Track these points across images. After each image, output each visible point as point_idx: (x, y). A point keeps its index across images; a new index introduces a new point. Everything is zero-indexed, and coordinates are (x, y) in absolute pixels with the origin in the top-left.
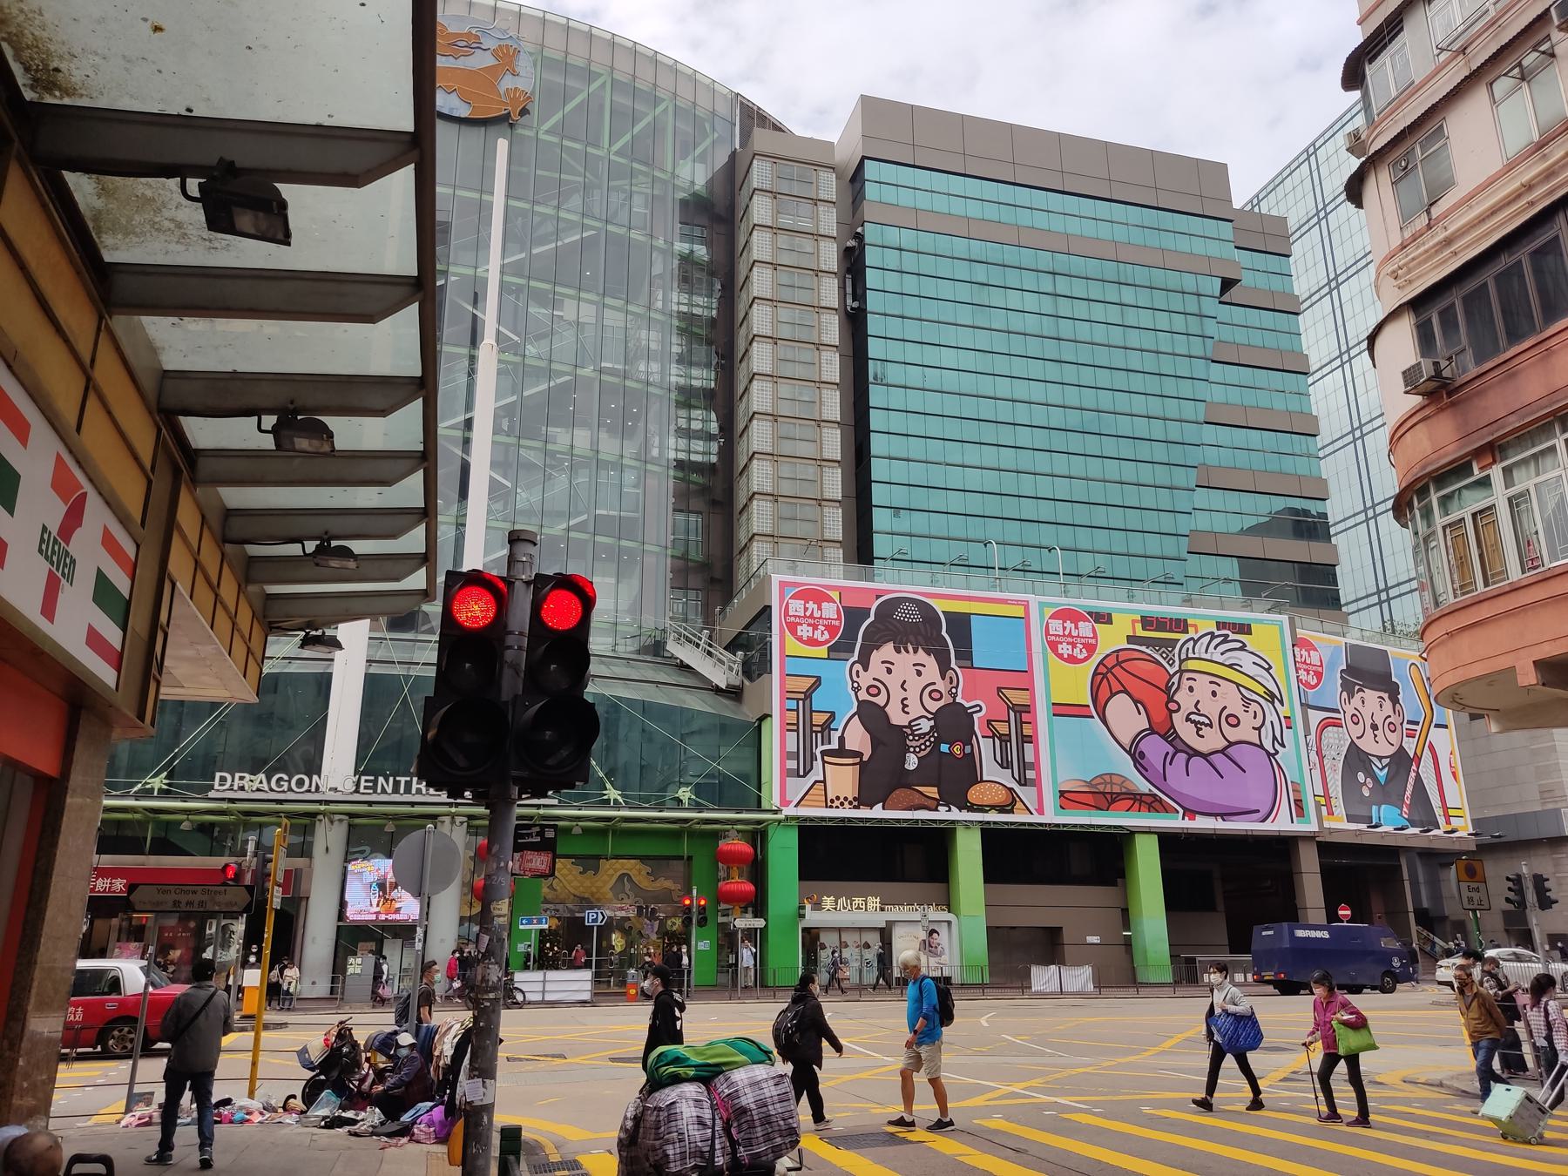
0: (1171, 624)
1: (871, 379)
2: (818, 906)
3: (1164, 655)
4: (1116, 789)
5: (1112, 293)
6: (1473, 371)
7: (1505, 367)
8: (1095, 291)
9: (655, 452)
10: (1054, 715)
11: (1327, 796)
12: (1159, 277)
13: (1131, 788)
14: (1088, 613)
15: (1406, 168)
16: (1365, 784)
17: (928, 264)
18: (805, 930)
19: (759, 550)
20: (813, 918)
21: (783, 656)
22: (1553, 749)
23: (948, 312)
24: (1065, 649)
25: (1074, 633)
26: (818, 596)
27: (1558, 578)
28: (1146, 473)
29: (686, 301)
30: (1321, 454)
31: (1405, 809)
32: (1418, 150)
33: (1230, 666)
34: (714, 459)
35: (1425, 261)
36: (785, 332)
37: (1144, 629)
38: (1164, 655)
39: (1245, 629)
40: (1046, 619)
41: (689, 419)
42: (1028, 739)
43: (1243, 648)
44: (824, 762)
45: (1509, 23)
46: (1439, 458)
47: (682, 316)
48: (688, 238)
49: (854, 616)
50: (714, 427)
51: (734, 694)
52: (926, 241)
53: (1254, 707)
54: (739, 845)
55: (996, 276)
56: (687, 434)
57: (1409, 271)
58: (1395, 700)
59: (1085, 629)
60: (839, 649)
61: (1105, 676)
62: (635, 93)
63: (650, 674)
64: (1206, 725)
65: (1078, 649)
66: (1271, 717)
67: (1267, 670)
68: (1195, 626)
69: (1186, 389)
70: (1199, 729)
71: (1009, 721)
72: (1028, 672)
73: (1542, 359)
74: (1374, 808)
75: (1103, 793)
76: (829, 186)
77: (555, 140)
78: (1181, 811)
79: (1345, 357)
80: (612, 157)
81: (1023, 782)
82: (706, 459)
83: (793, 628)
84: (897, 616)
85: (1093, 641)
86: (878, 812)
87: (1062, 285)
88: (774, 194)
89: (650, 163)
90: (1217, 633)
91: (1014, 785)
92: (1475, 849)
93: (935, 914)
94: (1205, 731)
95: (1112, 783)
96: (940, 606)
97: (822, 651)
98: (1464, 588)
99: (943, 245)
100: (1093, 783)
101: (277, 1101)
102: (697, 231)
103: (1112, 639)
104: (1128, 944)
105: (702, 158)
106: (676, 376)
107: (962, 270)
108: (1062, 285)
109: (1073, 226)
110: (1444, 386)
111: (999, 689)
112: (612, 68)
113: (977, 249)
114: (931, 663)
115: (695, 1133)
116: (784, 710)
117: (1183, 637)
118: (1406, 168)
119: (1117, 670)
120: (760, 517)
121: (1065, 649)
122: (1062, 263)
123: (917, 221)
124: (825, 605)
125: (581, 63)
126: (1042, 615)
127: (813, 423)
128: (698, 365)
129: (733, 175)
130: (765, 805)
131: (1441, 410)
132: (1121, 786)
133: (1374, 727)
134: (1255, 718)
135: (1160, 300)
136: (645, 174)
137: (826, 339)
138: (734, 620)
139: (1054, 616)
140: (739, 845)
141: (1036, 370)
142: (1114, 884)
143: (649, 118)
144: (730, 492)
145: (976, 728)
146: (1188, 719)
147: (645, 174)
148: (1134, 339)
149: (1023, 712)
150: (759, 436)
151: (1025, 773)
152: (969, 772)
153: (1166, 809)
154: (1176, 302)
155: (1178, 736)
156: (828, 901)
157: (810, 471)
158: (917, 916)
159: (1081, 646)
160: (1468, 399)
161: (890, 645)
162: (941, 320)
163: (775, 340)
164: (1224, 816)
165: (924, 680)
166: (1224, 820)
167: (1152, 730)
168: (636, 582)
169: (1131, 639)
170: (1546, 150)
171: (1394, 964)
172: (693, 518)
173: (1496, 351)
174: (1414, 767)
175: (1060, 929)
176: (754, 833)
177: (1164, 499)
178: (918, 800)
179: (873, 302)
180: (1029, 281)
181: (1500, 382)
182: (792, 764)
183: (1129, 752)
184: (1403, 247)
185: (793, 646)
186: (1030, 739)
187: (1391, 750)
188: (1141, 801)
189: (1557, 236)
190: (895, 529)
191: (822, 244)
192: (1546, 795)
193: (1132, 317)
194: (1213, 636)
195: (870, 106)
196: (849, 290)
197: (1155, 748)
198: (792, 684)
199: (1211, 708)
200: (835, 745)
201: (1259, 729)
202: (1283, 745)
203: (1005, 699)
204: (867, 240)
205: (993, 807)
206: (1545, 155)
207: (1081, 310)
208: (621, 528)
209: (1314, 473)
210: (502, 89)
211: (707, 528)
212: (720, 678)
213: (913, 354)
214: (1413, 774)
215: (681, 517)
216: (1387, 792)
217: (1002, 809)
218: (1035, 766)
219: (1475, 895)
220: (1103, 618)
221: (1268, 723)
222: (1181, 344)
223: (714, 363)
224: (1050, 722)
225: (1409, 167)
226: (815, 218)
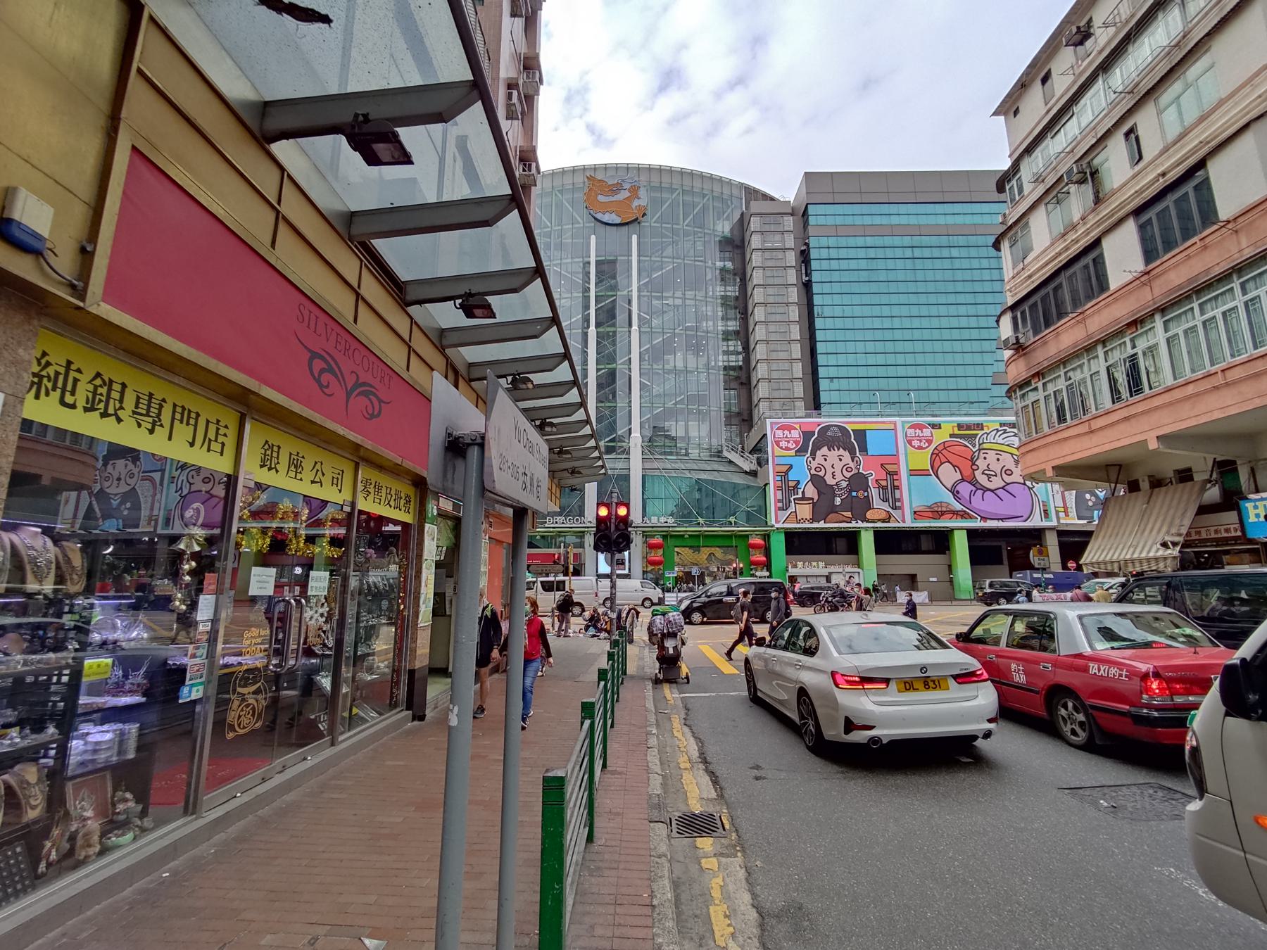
1: (816, 316)
2: (795, 566)
4: (944, 509)
5: (945, 253)
6: (1033, 340)
8: (936, 253)
9: (713, 363)
11: (1065, 507)
13: (953, 508)
14: (929, 425)
18: (789, 577)
19: (763, 406)
20: (792, 571)
24: (916, 443)
26: (790, 428)
33: (1008, 445)
36: (771, 300)
41: (728, 346)
47: (723, 297)
49: (807, 435)
50: (740, 349)
51: (754, 474)
54: (759, 541)
56: (727, 353)
59: (927, 432)
60: (801, 451)
61: (937, 455)
63: (716, 467)
68: (987, 426)
72: (896, 456)
76: (789, 222)
77: (659, 225)
78: (979, 518)
83: (777, 443)
84: (829, 433)
87: (917, 253)
88: (762, 233)
89: (702, 226)
93: (849, 569)
94: (993, 478)
95: (941, 507)
96: (849, 427)
98: (1029, 434)
99: (852, 241)
101: (577, 630)
103: (941, 437)
104: (951, 581)
105: (727, 218)
108: (917, 253)
110: (1021, 346)
113: (870, 241)
114: (846, 454)
115: (660, 625)
117: (981, 433)
120: (762, 391)
123: (837, 232)
125: (667, 186)
128: (730, 319)
129: (742, 223)
130: (769, 524)
131: (1021, 356)
132: (946, 507)
136: (700, 232)
137: (791, 300)
140: (759, 541)
142: (945, 553)
143: (701, 205)
145: (870, 484)
147: (700, 232)
149: (893, 474)
150: (760, 352)
151: (896, 504)
156: (800, 564)
157: (786, 366)
158: (841, 570)
161: (826, 448)
163: (765, 304)
167: (963, 480)
168: (708, 423)
169: (951, 436)
170: (1065, 237)
172: (732, 392)
173: (1041, 331)
175: (916, 575)
176: (765, 535)
178: (841, 518)
179: (816, 277)
180: (899, 253)
182: (780, 505)
184: (1013, 277)
185: (778, 452)
186: (897, 488)
190: (832, 389)
193: (957, 264)
194: (998, 430)
196: (804, 271)
197: (965, 489)
199: (996, 467)
200: (800, 495)
203: (886, 470)
204: (811, 246)
205: (879, 520)
207: (928, 264)
208: (700, 399)
210: (634, 207)
211: (739, 396)
212: (747, 466)
215: (727, 392)
217: (884, 521)
219: (1042, 562)
220: (936, 426)
224: (908, 480)
226: (783, 241)
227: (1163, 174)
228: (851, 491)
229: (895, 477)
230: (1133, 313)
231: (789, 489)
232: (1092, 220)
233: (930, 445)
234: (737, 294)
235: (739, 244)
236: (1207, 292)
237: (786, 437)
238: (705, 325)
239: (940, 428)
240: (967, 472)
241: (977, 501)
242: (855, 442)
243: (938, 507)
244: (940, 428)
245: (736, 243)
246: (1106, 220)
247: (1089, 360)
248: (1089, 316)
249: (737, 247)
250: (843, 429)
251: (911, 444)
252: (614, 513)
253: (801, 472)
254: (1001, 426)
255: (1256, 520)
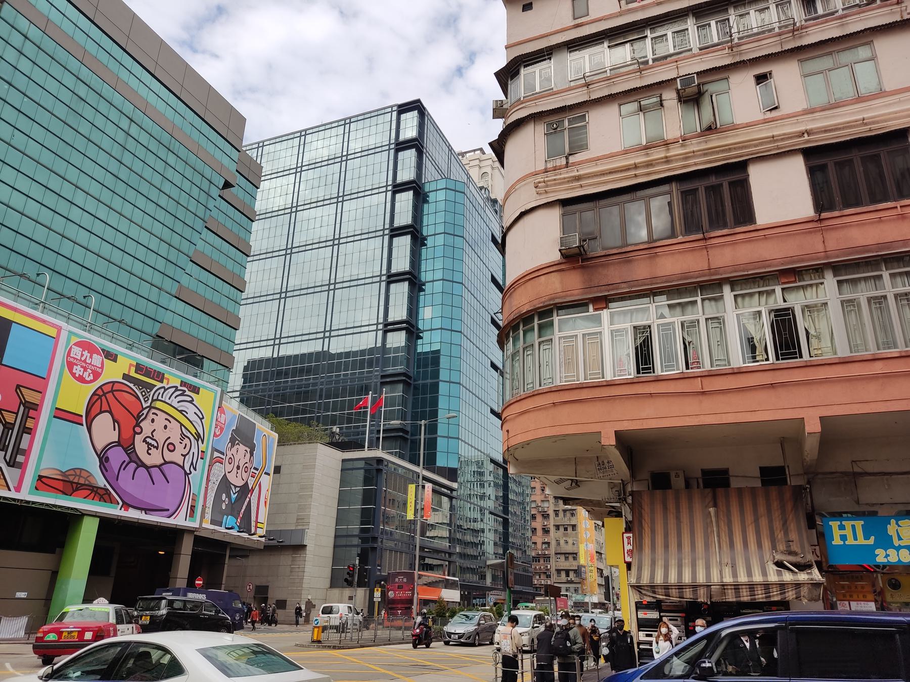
0: (154, 375)
3: (144, 394)
4: (82, 481)
7: (624, 256)
8: (153, 146)
10: (55, 417)
12: (192, 159)
13: (93, 482)
15: (556, 129)
16: (224, 501)
17: (44, 60)
22: (311, 496)
24: (78, 370)
25: (88, 361)
27: (641, 384)
28: (148, 273)
30: (243, 302)
31: (239, 520)
32: (566, 123)
33: (181, 411)
35: (560, 184)
37: (136, 372)
38: (144, 394)
39: (196, 390)
40: (72, 343)
42: (29, 431)
43: (191, 402)
45: (619, 83)
46: (567, 296)
52: (49, 45)
53: (186, 441)
55: (92, 98)
57: (547, 186)
58: (252, 454)
59: (97, 360)
61: (100, 397)
64: (154, 447)
65: (87, 373)
66: (194, 450)
67: (201, 419)
68: (168, 379)
69: (187, 233)
70: (149, 449)
71: (17, 414)
72: (45, 380)
73: (650, 258)
74: (225, 517)
75: (72, 483)
78: (121, 503)
79: (289, 251)
81: (11, 464)
85: (100, 370)
90: (180, 388)
92: (263, 548)
94: (153, 451)
95: (80, 476)
99: (61, 54)
100: (67, 473)
103: (113, 372)
109: (152, 99)
111: (18, 386)
117: (159, 385)
118: (556, 129)
119: (109, 396)
121: (78, 370)
122: (138, 116)
126: (69, 340)
131: (574, 268)
132: (86, 479)
133: (238, 468)
134: (184, 448)
135: (189, 173)
139: (77, 344)
141: (99, 173)
142: (53, 552)
146: (144, 441)
148: (167, 187)
149: (31, 409)
153: (112, 501)
154: (197, 179)
155: (135, 451)
159: (90, 372)
160: (596, 266)
164: (147, 510)
166: (146, 513)
167: (119, 443)
169: (125, 377)
171: (236, 618)
174: (249, 496)
177: (154, 294)
180: (114, 115)
181: (620, 263)
183: (98, 456)
184: (546, 171)
187: (241, 483)
188: (96, 492)
189: (698, 189)
192: (300, 521)
193: (170, 173)
197: (117, 456)
199: (160, 437)
201: (184, 456)
202: (195, 469)
203: (20, 395)
206: (648, 154)
209: (236, 313)
214: (248, 499)
216: (233, 509)
218: (26, 453)
220: (111, 356)
221: (191, 453)
222: (192, 206)
224: (49, 422)
225: (559, 129)
227: (809, 132)
230: (792, 259)
232: (695, 146)
233: (96, 378)
236: (895, 264)
239: (115, 360)
240: (127, 435)
241: (126, 482)
243: (76, 475)
244: (115, 360)
246: (718, 152)
247: (703, 300)
248: (714, 246)
251: (70, 370)
254: (181, 386)
255: (842, 543)
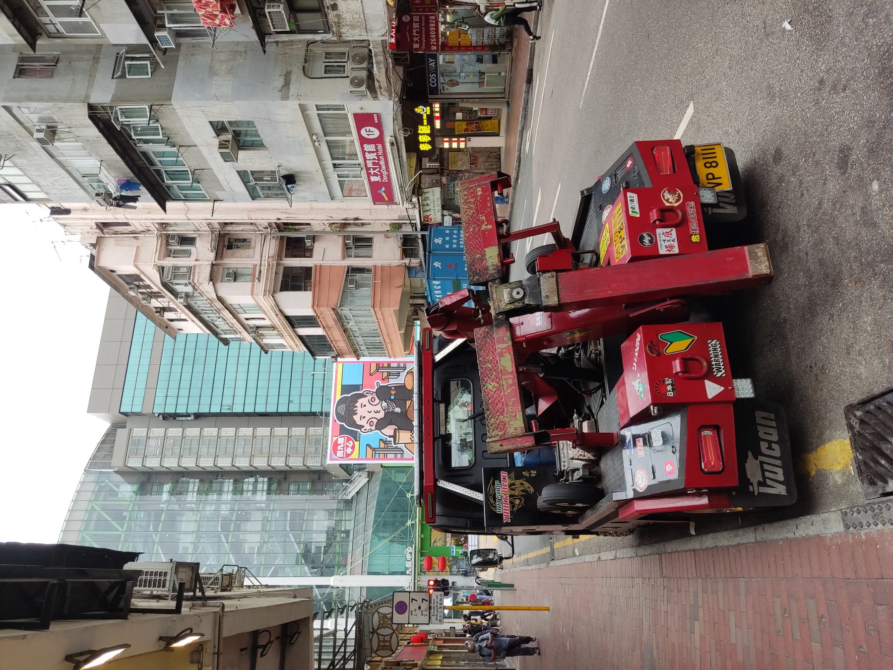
1: (230, 411)
9: (263, 505)
21: (359, 459)
23: (197, 375)
26: (336, 445)
29: (192, 493)
34: (266, 479)
36: (212, 451)
41: (248, 491)
44: (398, 444)
47: (199, 492)
48: (160, 492)
49: (343, 431)
50: (252, 480)
51: (371, 474)
52: (162, 384)
56: (255, 491)
60: (355, 436)
62: (89, 520)
80: (124, 530)
82: (266, 483)
83: (348, 455)
86: (415, 423)
91: (406, 371)
96: (339, 397)
97: (357, 443)
99: (163, 376)
102: (155, 488)
105: (118, 486)
106: (228, 497)
107: (177, 369)
111: (370, 375)
112: (80, 531)
113: (166, 361)
114: (361, 401)
116: (379, 459)
123: (151, 388)
124: (339, 443)
127: (254, 440)
129: (127, 474)
137: (215, 434)
138: (343, 474)
144: (281, 472)
152: (401, 388)
157: (276, 441)
161: (354, 417)
162: (201, 379)
165: (367, 404)
168: (316, 511)
172: (292, 487)
179: (193, 409)
182: (399, 456)
185: (355, 455)
186: (389, 364)
191: (169, 435)
195: (92, 409)
196: (184, 418)
198: (369, 456)
200: (392, 439)
204: (162, 412)
213: (218, 392)
218: (399, 363)
223: (221, 480)
226: (157, 438)
228: (390, 399)
229: (381, 365)
231: (386, 447)
234: (197, 480)
235: (147, 477)
237: (343, 448)
238: (224, 512)
242: (351, 395)
245: (145, 480)
249: (149, 478)
250: (340, 402)
252: (432, 587)
253: (372, 437)
